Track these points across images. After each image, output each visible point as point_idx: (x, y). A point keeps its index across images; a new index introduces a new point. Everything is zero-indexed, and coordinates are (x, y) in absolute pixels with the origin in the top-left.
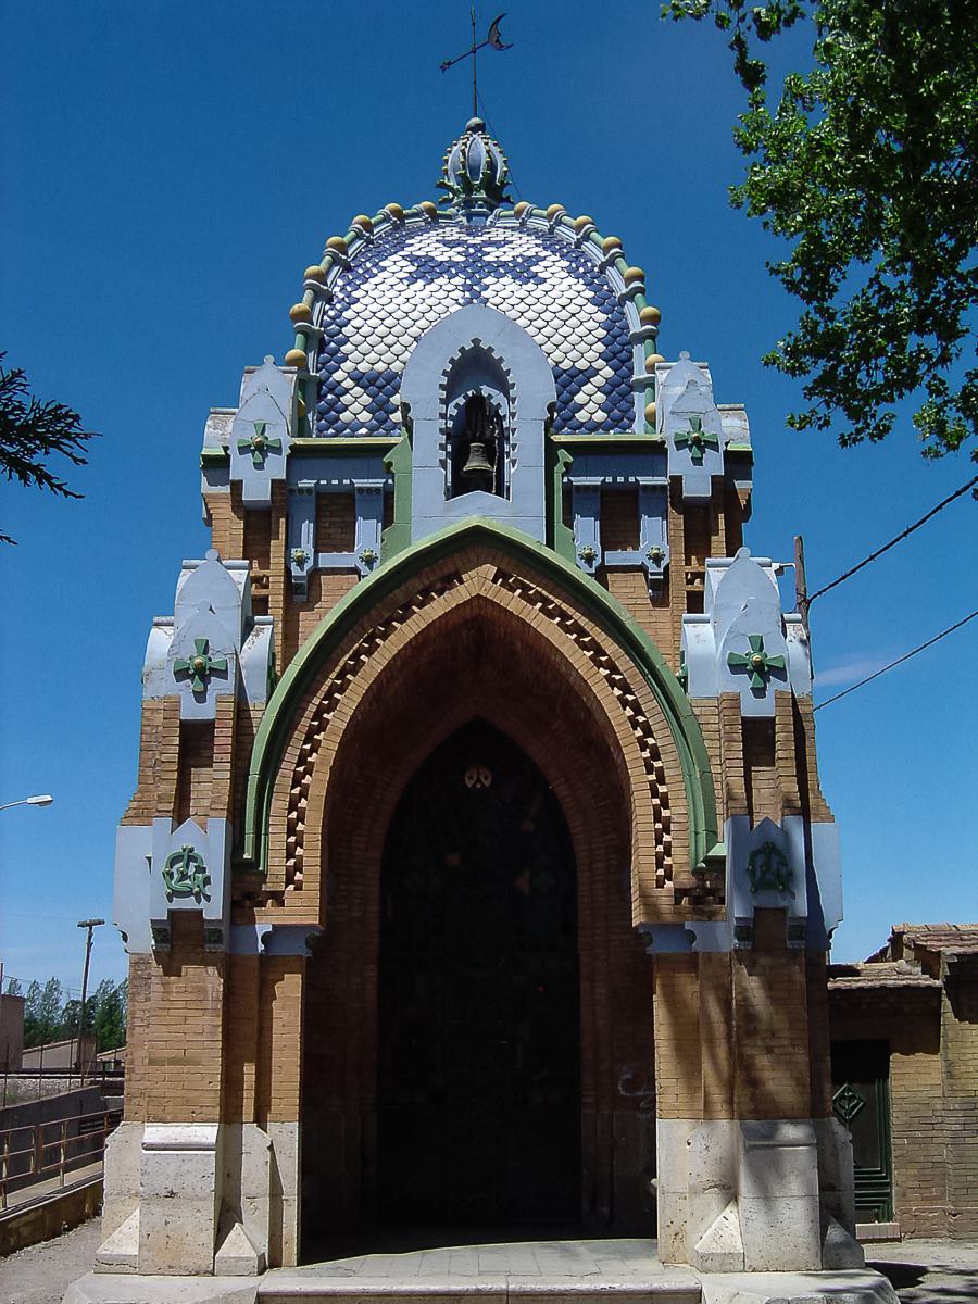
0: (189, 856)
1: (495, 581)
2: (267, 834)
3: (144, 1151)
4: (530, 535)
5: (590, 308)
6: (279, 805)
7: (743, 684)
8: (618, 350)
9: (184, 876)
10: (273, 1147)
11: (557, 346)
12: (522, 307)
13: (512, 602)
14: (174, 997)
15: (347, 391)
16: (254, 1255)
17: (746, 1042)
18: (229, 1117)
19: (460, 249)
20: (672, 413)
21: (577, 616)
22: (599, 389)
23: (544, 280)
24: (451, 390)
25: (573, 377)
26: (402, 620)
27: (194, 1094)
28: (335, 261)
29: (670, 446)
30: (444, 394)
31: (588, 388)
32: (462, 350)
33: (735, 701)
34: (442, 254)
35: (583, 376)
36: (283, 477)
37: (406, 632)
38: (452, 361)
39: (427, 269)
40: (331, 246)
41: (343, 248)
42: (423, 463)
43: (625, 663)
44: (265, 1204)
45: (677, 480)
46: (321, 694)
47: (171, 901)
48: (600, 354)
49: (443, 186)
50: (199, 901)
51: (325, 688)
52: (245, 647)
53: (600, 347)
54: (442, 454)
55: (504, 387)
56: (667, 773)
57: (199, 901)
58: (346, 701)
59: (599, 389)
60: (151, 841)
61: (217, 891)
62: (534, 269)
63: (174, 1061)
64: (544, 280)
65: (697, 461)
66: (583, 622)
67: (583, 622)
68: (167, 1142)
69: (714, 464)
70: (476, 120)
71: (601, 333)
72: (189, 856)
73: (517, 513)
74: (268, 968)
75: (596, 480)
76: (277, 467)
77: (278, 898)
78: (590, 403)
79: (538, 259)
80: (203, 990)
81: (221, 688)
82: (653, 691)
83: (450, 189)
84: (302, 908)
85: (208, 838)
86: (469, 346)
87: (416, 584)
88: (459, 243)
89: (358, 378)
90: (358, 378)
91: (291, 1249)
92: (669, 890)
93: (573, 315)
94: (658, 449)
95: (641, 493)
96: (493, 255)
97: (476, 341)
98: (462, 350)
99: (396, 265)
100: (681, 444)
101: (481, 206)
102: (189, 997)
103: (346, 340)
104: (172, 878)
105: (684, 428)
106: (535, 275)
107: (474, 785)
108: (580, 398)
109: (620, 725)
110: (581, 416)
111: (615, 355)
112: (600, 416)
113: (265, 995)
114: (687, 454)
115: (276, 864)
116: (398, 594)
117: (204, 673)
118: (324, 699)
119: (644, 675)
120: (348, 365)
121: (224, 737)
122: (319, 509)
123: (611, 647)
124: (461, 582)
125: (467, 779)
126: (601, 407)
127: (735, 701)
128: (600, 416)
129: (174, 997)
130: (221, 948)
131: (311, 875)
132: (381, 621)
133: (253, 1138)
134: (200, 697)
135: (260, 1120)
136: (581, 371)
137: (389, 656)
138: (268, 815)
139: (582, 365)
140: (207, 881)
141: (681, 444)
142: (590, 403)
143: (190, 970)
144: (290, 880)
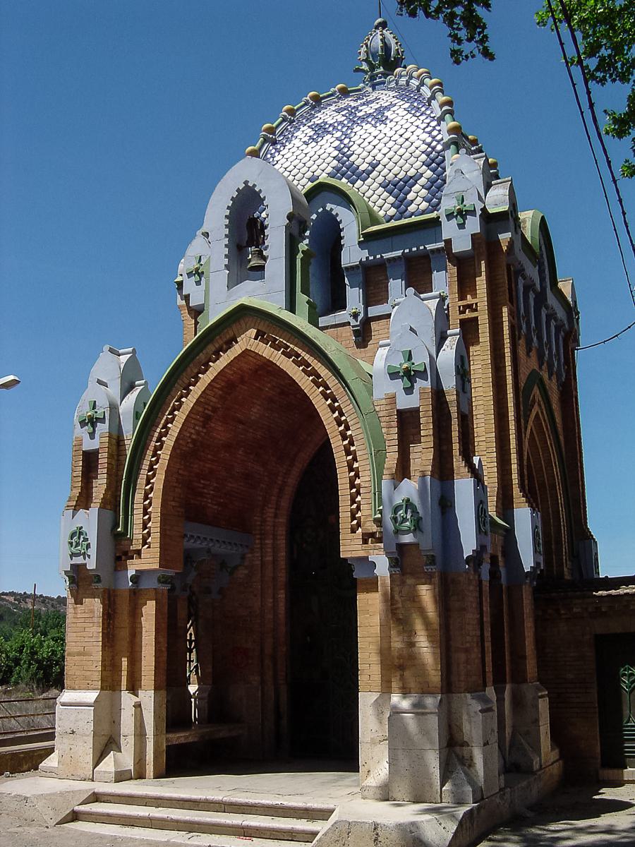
0: (79, 533)
1: (256, 338)
2: (132, 515)
3: (61, 707)
4: (274, 305)
6: (139, 496)
7: (398, 386)
9: (78, 544)
10: (141, 706)
11: (396, 163)
12: (376, 142)
13: (266, 351)
16: (113, 770)
21: (303, 354)
22: (423, 187)
25: (406, 182)
26: (203, 373)
27: (89, 673)
28: (266, 140)
29: (443, 219)
31: (417, 187)
35: (410, 181)
37: (206, 379)
39: (321, 130)
40: (264, 131)
41: (271, 131)
43: (332, 382)
44: (131, 740)
45: (448, 242)
46: (161, 426)
47: (72, 559)
48: (423, 162)
49: (358, 70)
50: (85, 559)
51: (163, 422)
52: (124, 401)
56: (358, 453)
57: (85, 559)
58: (174, 428)
59: (423, 187)
60: (68, 523)
61: (93, 552)
63: (79, 654)
65: (461, 226)
66: (307, 357)
67: (307, 357)
68: (74, 701)
69: (474, 225)
70: (379, 20)
72: (79, 533)
73: (266, 294)
74: (136, 598)
75: (399, 253)
77: (139, 552)
80: (92, 611)
81: (103, 428)
82: (350, 399)
83: (363, 71)
84: (148, 560)
85: (89, 520)
86: (242, 186)
87: (211, 348)
92: (359, 534)
93: (407, 140)
94: (436, 222)
95: (431, 256)
97: (246, 183)
98: (238, 190)
99: (304, 132)
100: (450, 216)
101: (380, 78)
102: (86, 615)
104: (72, 546)
108: (410, 197)
109: (329, 424)
110: (412, 208)
111: (433, 161)
112: (424, 205)
113: (135, 614)
114: (454, 222)
115: (137, 533)
116: (202, 356)
117: (92, 422)
118: (162, 428)
119: (344, 388)
121: (103, 459)
123: (324, 372)
124: (237, 342)
126: (424, 199)
128: (424, 205)
130: (100, 585)
131: (155, 539)
132: (192, 375)
133: (127, 699)
134: (92, 435)
135: (134, 688)
136: (411, 177)
137: (197, 396)
138: (133, 503)
139: (412, 172)
140: (88, 546)
141: (450, 216)
142: (418, 198)
143: (86, 601)
144: (145, 543)
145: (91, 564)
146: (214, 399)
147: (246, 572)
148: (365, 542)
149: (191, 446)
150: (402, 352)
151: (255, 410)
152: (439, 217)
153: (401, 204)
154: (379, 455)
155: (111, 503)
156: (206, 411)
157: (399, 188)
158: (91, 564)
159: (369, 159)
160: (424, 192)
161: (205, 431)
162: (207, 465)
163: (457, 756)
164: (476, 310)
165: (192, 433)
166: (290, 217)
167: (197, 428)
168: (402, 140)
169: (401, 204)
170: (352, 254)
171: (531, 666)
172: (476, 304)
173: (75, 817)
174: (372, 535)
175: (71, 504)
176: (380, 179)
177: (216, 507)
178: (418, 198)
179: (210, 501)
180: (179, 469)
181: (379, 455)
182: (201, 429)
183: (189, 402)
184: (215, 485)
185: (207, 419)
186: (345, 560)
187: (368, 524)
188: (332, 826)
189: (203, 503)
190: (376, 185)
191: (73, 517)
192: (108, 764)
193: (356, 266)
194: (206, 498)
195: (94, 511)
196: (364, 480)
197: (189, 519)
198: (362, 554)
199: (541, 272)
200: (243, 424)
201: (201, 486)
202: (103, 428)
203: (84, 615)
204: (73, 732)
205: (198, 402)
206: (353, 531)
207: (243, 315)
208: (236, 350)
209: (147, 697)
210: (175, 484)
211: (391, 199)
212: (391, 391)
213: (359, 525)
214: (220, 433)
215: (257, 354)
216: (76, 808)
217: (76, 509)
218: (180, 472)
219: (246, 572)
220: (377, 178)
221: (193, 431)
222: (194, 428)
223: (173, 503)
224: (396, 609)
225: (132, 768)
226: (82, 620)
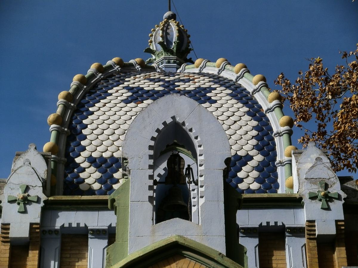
5: (247, 118)
15: (83, 170)
19: (161, 83)
20: (306, 179)
23: (215, 102)
24: (156, 159)
29: (306, 200)
30: (151, 162)
32: (165, 123)
34: (147, 86)
36: (38, 220)
38: (158, 131)
42: (137, 188)
53: (254, 142)
54: (151, 193)
55: (194, 156)
62: (208, 95)
64: (215, 102)
71: (255, 133)
76: (35, 213)
78: (248, 179)
79: (211, 89)
86: (169, 121)
88: (159, 80)
89: (92, 161)
90: (92, 161)
97: (173, 118)
99: (118, 93)
100: (313, 198)
103: (85, 137)
105: (316, 189)
106: (210, 98)
108: (240, 175)
112: (255, 186)
120: (84, 154)
122: (63, 245)
126: (257, 180)
139: (241, 153)
152: (301, 199)
160: (255, 174)
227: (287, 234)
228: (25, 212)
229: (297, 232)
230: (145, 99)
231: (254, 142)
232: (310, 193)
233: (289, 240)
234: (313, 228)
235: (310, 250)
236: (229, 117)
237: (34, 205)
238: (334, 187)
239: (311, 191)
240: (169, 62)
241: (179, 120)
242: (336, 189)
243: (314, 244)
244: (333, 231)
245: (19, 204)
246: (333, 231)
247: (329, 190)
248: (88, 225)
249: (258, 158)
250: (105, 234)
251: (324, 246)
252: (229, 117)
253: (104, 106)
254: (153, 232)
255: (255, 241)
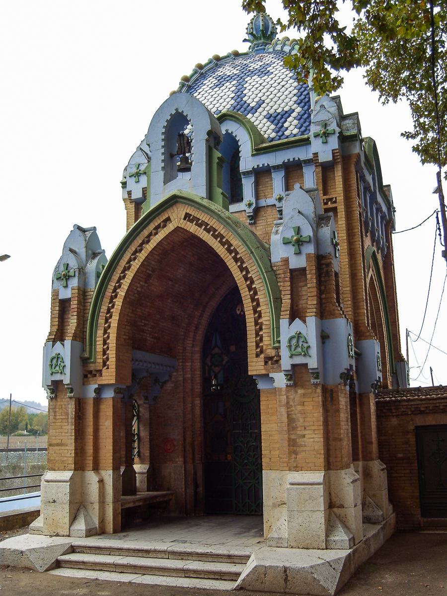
0: (58, 357)
1: (185, 219)
3: (45, 483)
6: (100, 332)
8: (304, 101)
12: (261, 88)
13: (192, 228)
14: (58, 417)
17: (292, 433)
18: (79, 467)
29: (312, 139)
31: (289, 119)
33: (286, 261)
35: (286, 114)
39: (221, 81)
44: (96, 506)
56: (261, 300)
61: (68, 370)
63: (58, 445)
65: (325, 143)
77: (100, 372)
85: (65, 350)
86: (174, 112)
91: (110, 527)
96: (253, 66)
99: (210, 81)
100: (316, 136)
101: (262, 46)
102: (63, 417)
107: (240, 314)
108: (286, 125)
109: (239, 280)
110: (287, 133)
112: (296, 131)
114: (320, 140)
121: (74, 304)
125: (237, 311)
127: (286, 261)
128: (296, 131)
129: (58, 417)
133: (92, 478)
135: (96, 468)
137: (141, 260)
138: (96, 336)
139: (287, 109)
141: (316, 136)
145: (66, 380)
146: (153, 263)
147: (173, 385)
148: (266, 363)
149: (136, 295)
150: (293, 228)
151: (180, 271)
152: (309, 138)
153: (280, 129)
154: (278, 301)
155: (79, 336)
156: (148, 271)
157: (278, 119)
158: (66, 380)
159: (257, 99)
160: (296, 122)
161: (146, 285)
162: (147, 310)
163: (336, 515)
164: (335, 202)
165: (137, 287)
166: (209, 133)
167: (141, 283)
168: (279, 87)
169: (280, 129)
170: (247, 162)
171: (375, 447)
172: (336, 198)
173: (58, 564)
174: (271, 358)
175: (51, 337)
176: (265, 113)
177: (151, 340)
178: (292, 128)
179: (148, 335)
180: (129, 312)
181: (278, 301)
182: (144, 284)
183: (136, 265)
184: (152, 324)
185: (148, 277)
186: (252, 376)
187: (269, 351)
188: (253, 569)
189: (144, 337)
190: (261, 117)
191: (53, 346)
192: (81, 525)
193: (250, 171)
194: (146, 333)
195: (68, 342)
196: (266, 319)
197: (134, 348)
198: (264, 372)
199: (374, 179)
200: (172, 281)
201: (143, 324)
202: (74, 282)
203: (61, 417)
204: (54, 501)
205: (142, 265)
206: (257, 356)
207: (173, 201)
208: (171, 227)
209: (108, 475)
210: (126, 323)
211: (273, 127)
212: (285, 255)
213: (262, 352)
214: (157, 287)
215: (186, 230)
216: (59, 558)
217: (54, 342)
218: (129, 314)
219: (173, 385)
220: (263, 112)
221: (138, 285)
222: (139, 283)
223: (124, 337)
224: (292, 411)
225: (98, 526)
226: (60, 421)
227: (303, 165)
228: (138, 182)
229: (308, 162)
230: (167, 101)
231: (295, 98)
232: (314, 133)
233: (274, 175)
234: (317, 158)
235: (317, 174)
236: (279, 83)
237: (333, 136)
238: (332, 125)
239: (316, 131)
240: (258, 47)
241: (180, 111)
242: (333, 126)
243: (320, 169)
244: (330, 158)
245: (135, 177)
246: (330, 158)
247: (328, 128)
248: (300, 158)
249: (299, 109)
250: (282, 168)
251: (326, 169)
252: (279, 83)
253: (198, 94)
254: (164, 190)
255: (253, 179)
